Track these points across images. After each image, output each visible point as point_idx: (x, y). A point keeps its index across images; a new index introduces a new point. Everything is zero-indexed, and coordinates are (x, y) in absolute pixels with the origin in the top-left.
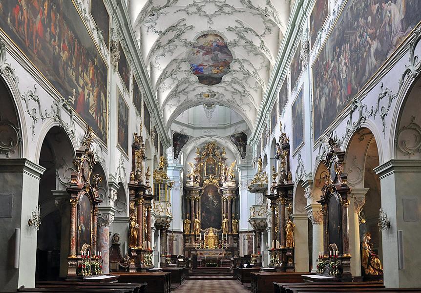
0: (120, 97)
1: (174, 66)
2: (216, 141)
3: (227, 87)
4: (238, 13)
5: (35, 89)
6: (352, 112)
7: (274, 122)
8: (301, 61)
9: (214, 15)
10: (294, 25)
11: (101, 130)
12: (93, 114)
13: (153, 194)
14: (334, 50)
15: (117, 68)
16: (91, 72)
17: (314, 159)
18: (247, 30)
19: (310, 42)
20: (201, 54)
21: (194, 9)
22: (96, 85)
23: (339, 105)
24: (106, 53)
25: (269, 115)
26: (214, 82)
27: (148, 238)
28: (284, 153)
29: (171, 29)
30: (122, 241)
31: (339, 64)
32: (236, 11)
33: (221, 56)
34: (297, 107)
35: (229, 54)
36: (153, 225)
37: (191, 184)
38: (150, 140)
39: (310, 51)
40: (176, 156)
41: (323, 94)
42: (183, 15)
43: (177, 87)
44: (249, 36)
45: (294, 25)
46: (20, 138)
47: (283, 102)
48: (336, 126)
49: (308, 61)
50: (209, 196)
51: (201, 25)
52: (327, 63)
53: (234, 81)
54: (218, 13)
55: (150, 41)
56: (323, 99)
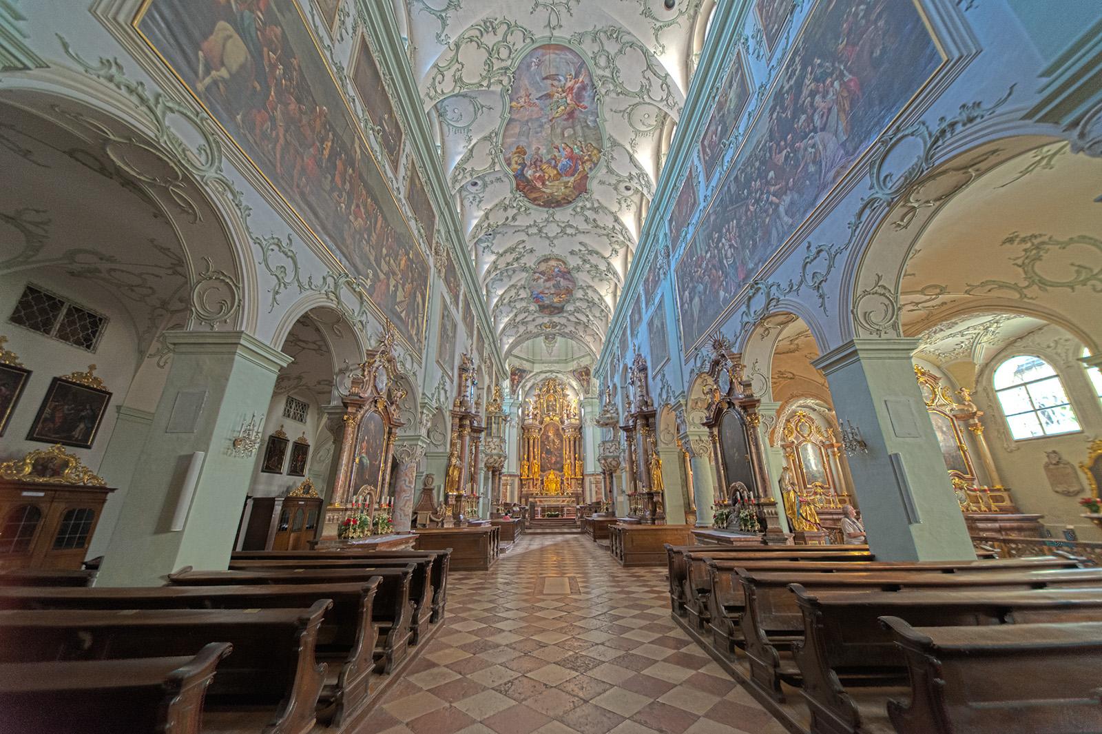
0: (445, 307)
1: (513, 292)
2: (557, 377)
3: (570, 317)
4: (583, 235)
5: (290, 240)
6: (750, 298)
7: (624, 345)
8: (659, 269)
9: (555, 237)
10: (648, 235)
11: (414, 336)
12: (401, 312)
13: (484, 425)
14: (710, 237)
15: (443, 275)
16: (403, 262)
17: (686, 377)
18: (591, 252)
19: (670, 246)
20: (542, 280)
21: (534, 230)
22: (409, 281)
23: (725, 298)
24: (428, 252)
25: (617, 341)
26: (556, 311)
27: (473, 478)
28: (642, 375)
29: (512, 250)
30: (438, 482)
31: (720, 251)
32: (580, 232)
33: (563, 283)
34: (657, 322)
35: (573, 281)
36: (482, 465)
37: (531, 421)
38: (483, 367)
39: (671, 255)
40: (513, 392)
41: (695, 294)
42: (523, 237)
43: (516, 316)
44: (594, 259)
45: (648, 235)
46: (240, 300)
47: (634, 324)
48: (722, 323)
49: (669, 266)
50: (550, 434)
51: (543, 249)
52: (698, 259)
53: (578, 310)
54: (561, 235)
55: (488, 260)
56: (697, 300)
